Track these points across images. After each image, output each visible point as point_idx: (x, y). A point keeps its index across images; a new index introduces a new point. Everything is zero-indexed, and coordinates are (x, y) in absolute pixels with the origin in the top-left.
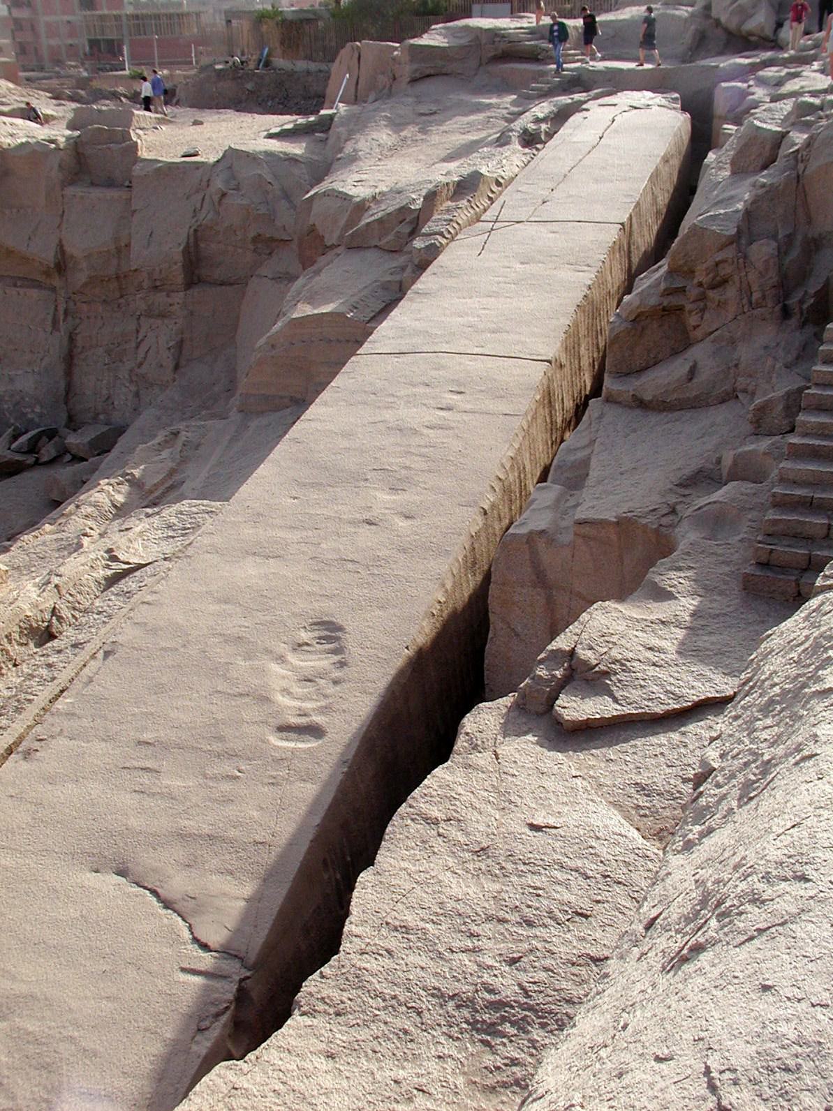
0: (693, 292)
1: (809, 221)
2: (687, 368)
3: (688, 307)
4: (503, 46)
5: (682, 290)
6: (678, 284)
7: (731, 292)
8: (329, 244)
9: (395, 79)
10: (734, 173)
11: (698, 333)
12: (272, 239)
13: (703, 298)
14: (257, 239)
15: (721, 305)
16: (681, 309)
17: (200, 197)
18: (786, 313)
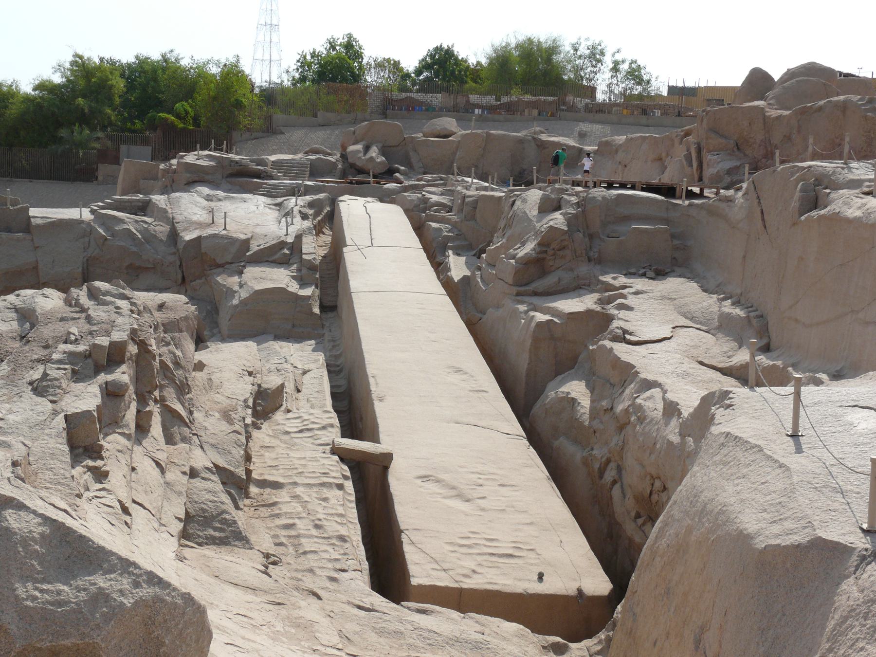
0: (551, 252)
1: (587, 227)
2: (556, 279)
3: (549, 258)
4: (238, 168)
5: (546, 252)
6: (544, 249)
7: (567, 252)
8: (219, 261)
9: (173, 181)
10: (539, 212)
11: (553, 269)
12: (140, 268)
13: (554, 255)
14: (130, 266)
15: (563, 257)
16: (544, 259)
17: (87, 239)
18: (590, 260)
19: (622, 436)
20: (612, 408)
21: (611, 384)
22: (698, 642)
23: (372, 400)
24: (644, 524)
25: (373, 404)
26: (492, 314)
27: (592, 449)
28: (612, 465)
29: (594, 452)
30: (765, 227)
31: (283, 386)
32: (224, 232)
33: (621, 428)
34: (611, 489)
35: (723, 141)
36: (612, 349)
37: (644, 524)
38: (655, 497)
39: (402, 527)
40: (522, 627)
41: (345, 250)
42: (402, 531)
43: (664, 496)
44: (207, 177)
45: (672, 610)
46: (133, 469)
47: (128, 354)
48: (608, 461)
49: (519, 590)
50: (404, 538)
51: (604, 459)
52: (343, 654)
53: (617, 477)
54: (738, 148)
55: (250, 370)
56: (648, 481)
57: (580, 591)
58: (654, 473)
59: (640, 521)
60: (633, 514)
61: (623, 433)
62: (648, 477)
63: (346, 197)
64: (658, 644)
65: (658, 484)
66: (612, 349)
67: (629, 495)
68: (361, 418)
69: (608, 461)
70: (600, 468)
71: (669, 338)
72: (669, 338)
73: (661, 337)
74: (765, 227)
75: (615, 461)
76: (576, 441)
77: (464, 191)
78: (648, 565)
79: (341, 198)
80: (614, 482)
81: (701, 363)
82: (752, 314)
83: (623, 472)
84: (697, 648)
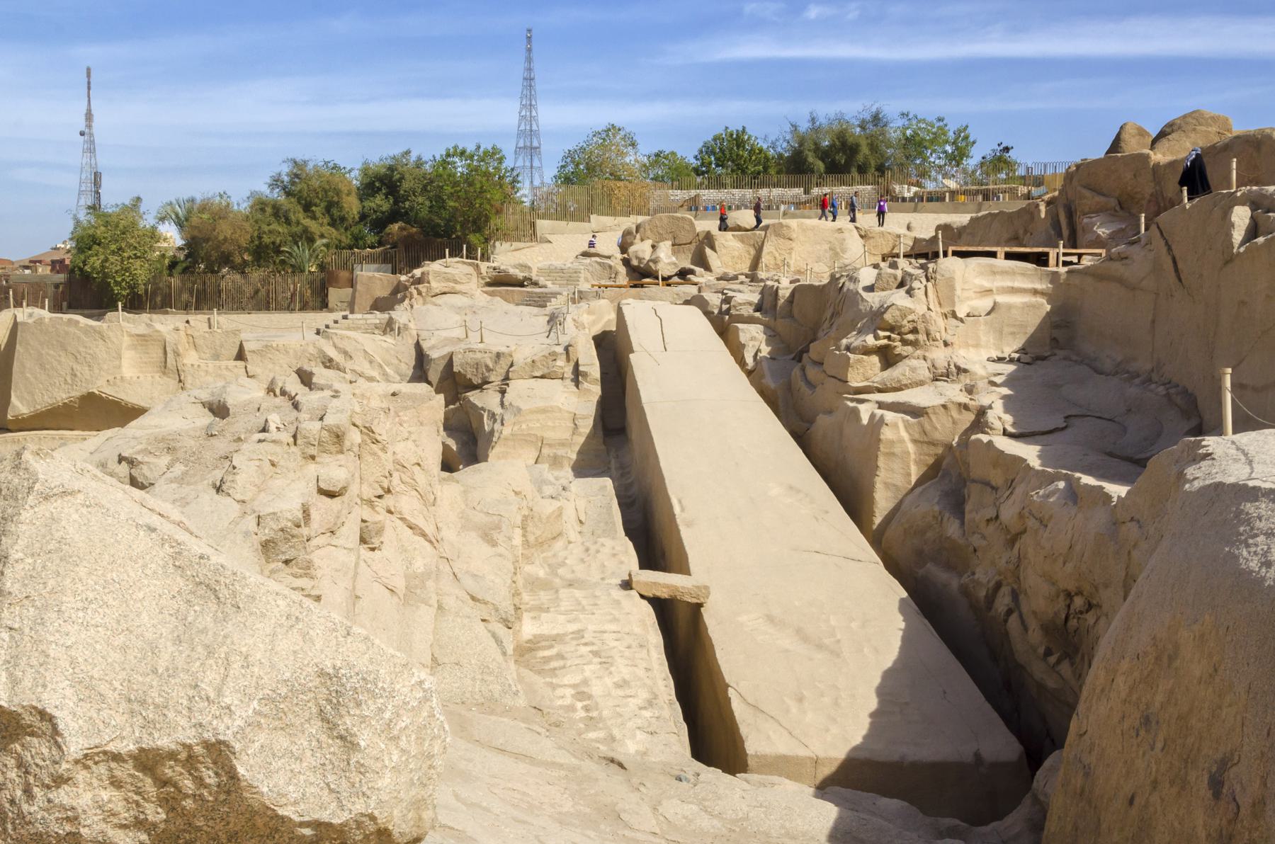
19: (1016, 550)
20: (997, 517)
21: (993, 488)
22: (1216, 785)
23: (677, 526)
24: (1059, 662)
25: (678, 531)
26: (823, 421)
27: (974, 574)
28: (1005, 590)
29: (976, 576)
30: (1180, 280)
31: (560, 509)
32: (481, 346)
33: (1012, 540)
34: (1006, 621)
35: (1102, 199)
36: (990, 442)
37: (1059, 662)
38: (1073, 623)
39: (728, 679)
40: (906, 804)
41: (631, 356)
42: (728, 686)
43: (1090, 618)
44: (458, 287)
45: (1159, 745)
46: (357, 597)
47: (347, 444)
48: (998, 585)
49: (896, 758)
50: (731, 693)
51: (992, 584)
52: (663, 841)
53: (1012, 605)
54: (1122, 208)
55: (517, 490)
56: (1061, 603)
57: (977, 755)
58: (1071, 586)
59: (1052, 659)
60: (1041, 650)
61: (1017, 546)
62: (1062, 598)
63: (630, 300)
64: (1137, 801)
65: (1078, 602)
66: (990, 442)
67: (1033, 625)
68: (663, 554)
69: (998, 585)
70: (986, 596)
71: (1063, 429)
72: (1063, 429)
73: (1052, 427)
74: (1180, 280)
75: (1008, 584)
76: (949, 567)
77: (776, 284)
78: (1103, 690)
79: (624, 301)
80: (1009, 612)
81: (1111, 454)
82: (1172, 391)
83: (1022, 597)
84: (1217, 795)
